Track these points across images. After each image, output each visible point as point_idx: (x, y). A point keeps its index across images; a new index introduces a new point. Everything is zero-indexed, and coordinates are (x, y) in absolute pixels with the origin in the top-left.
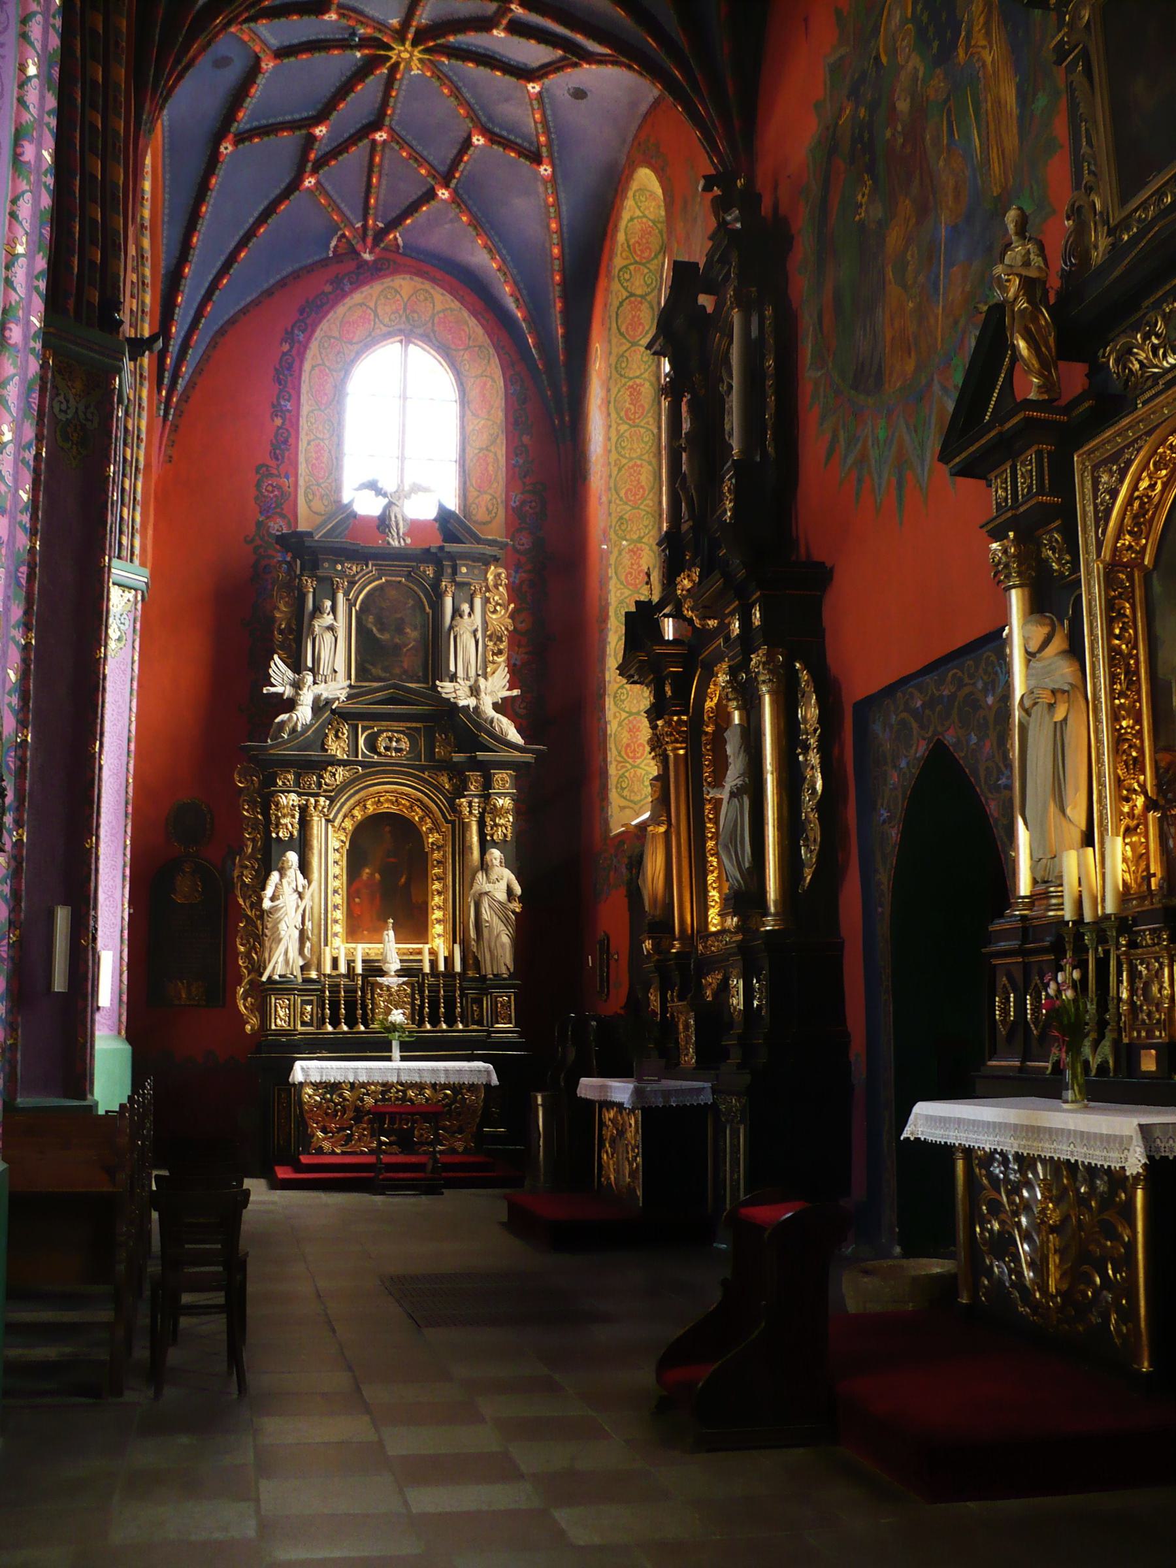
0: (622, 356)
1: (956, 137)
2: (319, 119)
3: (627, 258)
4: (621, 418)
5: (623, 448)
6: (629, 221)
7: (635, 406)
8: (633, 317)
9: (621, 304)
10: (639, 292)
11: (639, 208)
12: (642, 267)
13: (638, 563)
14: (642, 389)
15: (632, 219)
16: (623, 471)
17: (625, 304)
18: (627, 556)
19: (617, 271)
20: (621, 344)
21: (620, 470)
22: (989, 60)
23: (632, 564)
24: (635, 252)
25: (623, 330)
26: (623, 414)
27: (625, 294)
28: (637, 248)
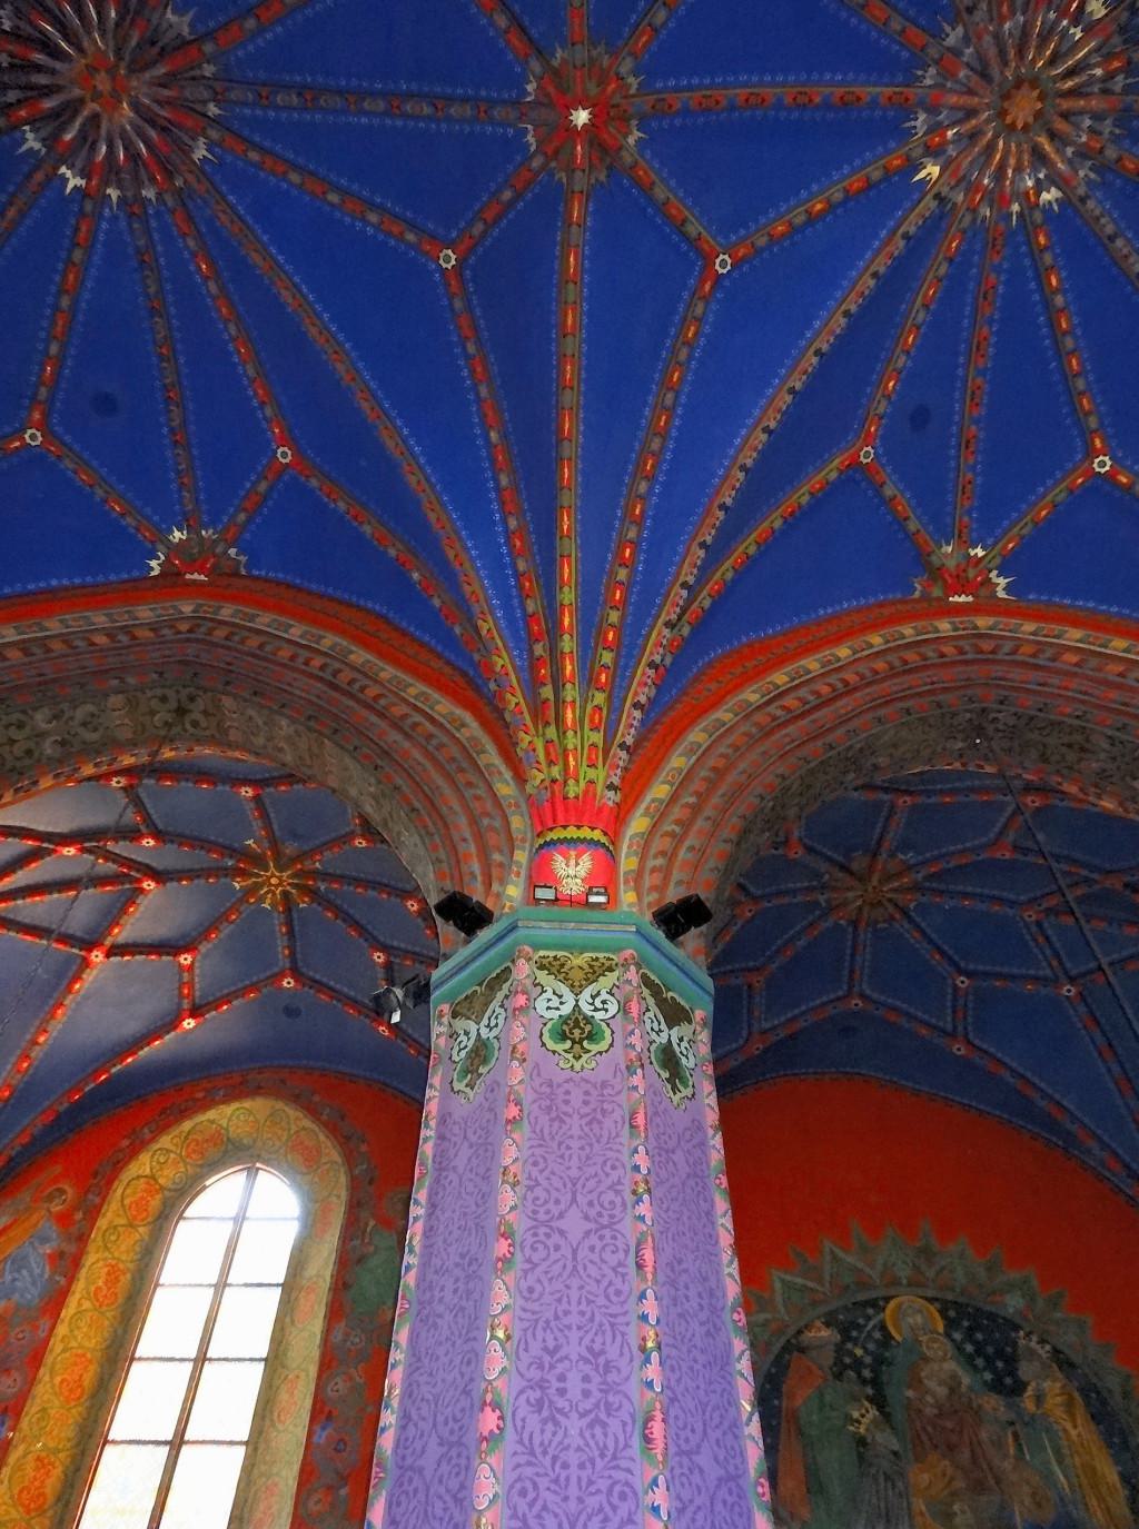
0: (115, 1227)
1: (1028, 1457)
2: (158, 835)
3: (176, 1145)
4: (88, 1293)
5: (78, 1328)
6: (208, 1120)
7: (109, 1289)
8: (142, 1198)
9: (138, 1177)
10: (161, 1181)
11: (230, 1120)
12: (181, 1165)
13: (43, 1482)
14: (122, 1278)
15: (212, 1122)
16: (67, 1355)
17: (142, 1180)
18: (33, 1464)
19: (158, 1146)
20: (119, 1216)
21: (64, 1351)
22: (1073, 1433)
23: (35, 1478)
24: (188, 1146)
25: (127, 1202)
26: (93, 1288)
27: (148, 1171)
28: (192, 1146)
